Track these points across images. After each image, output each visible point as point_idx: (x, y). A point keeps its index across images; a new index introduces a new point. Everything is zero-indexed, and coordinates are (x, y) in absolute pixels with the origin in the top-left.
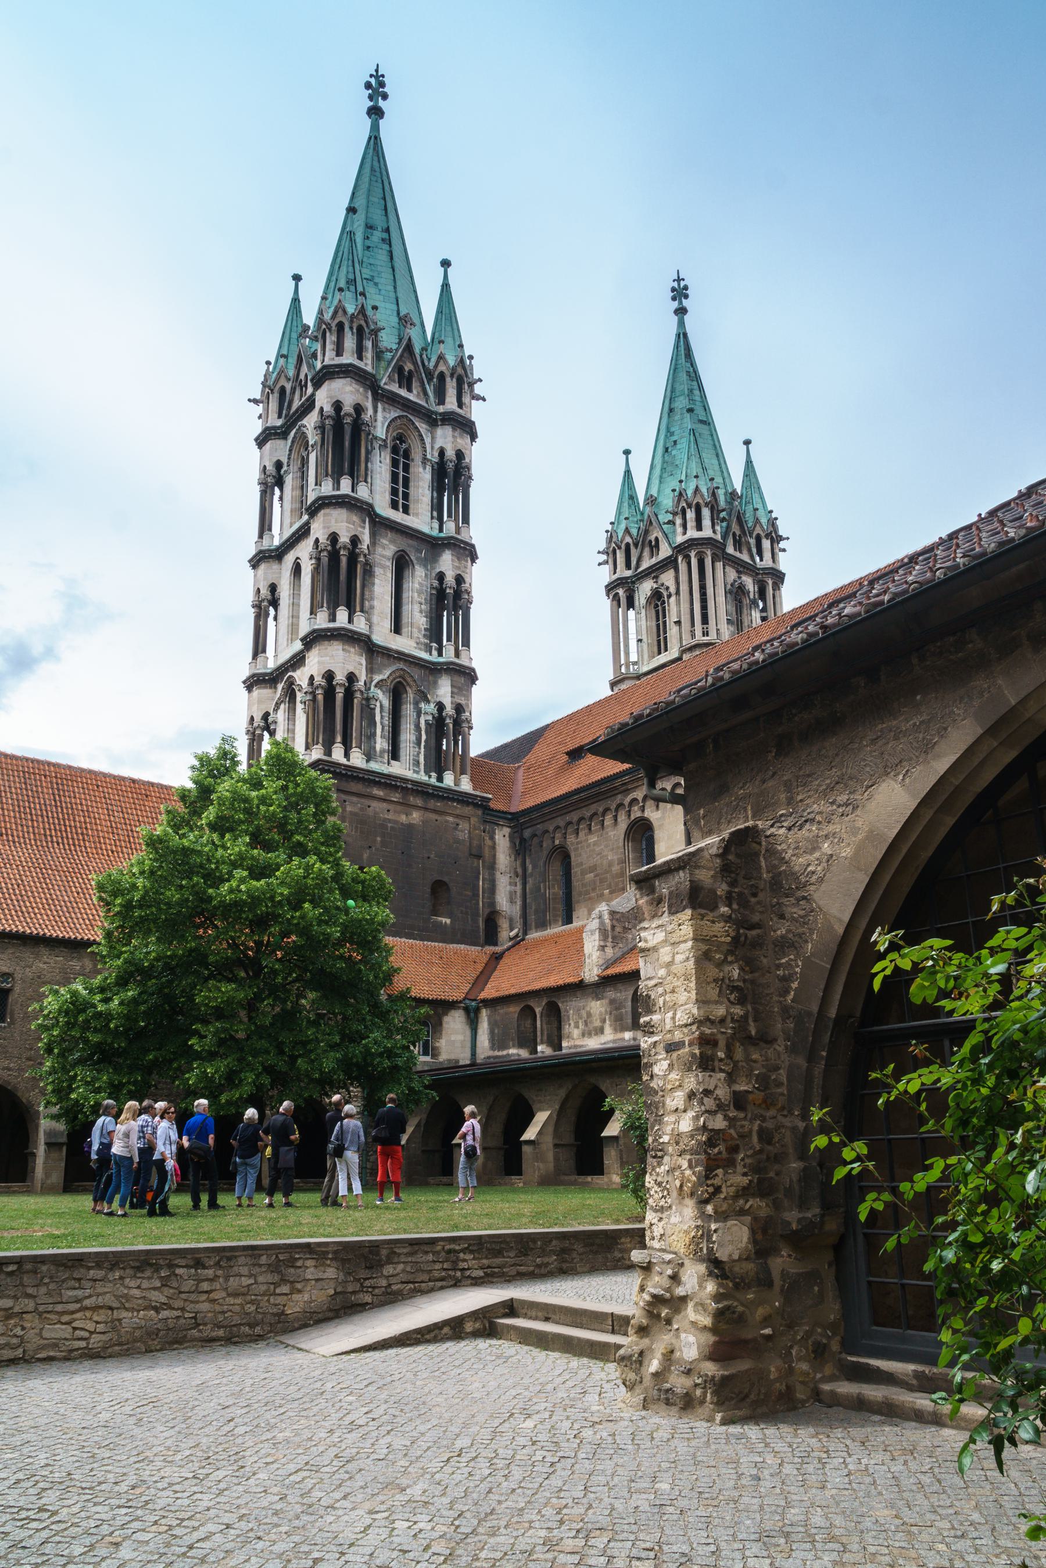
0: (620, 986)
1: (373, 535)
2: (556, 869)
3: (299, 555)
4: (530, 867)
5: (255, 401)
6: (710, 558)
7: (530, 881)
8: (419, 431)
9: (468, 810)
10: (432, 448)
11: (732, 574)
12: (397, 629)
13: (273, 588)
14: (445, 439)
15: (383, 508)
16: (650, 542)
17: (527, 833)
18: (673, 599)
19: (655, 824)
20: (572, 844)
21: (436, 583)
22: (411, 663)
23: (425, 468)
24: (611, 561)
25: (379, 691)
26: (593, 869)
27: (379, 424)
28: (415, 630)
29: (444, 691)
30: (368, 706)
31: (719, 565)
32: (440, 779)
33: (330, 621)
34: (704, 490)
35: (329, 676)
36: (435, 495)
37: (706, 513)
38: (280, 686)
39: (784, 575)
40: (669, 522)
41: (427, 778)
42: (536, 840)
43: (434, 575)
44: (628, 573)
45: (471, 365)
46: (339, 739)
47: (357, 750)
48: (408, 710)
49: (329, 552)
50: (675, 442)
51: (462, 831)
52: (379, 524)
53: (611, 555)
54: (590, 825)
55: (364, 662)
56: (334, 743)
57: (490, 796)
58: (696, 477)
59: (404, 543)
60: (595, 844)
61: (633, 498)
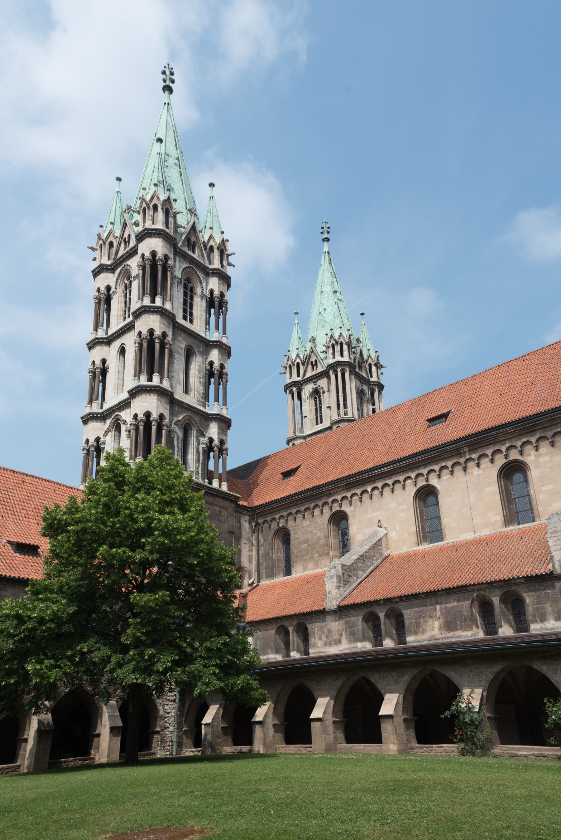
0: (353, 612)
2: (279, 544)
4: (262, 541)
7: (262, 549)
9: (227, 504)
11: (359, 384)
12: (186, 391)
13: (104, 361)
16: (312, 362)
17: (260, 521)
18: (325, 395)
19: (349, 514)
20: (292, 526)
21: (208, 368)
22: (195, 412)
25: (176, 427)
26: (306, 541)
29: (213, 430)
30: (170, 436)
31: (353, 377)
32: (210, 483)
35: (148, 415)
37: (345, 347)
39: (384, 386)
40: (323, 352)
41: (203, 482)
42: (266, 525)
43: (207, 362)
44: (299, 379)
48: (193, 441)
50: (325, 309)
51: (223, 516)
53: (288, 369)
54: (304, 515)
55: (168, 408)
57: (240, 496)
59: (192, 342)
60: (308, 526)
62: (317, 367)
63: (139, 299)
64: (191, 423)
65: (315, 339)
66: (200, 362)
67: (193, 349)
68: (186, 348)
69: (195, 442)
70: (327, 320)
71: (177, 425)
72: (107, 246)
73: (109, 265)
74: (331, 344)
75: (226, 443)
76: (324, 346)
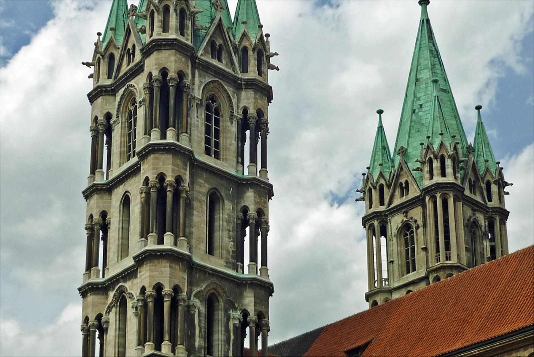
1: (192, 176)
3: (129, 189)
6: (452, 199)
8: (228, 93)
10: (238, 107)
11: (469, 212)
12: (211, 251)
13: (104, 215)
16: (401, 184)
21: (241, 215)
22: (222, 278)
23: (232, 123)
24: (367, 197)
25: (197, 300)
28: (224, 252)
33: (158, 244)
35: (159, 287)
36: (240, 144)
37: (449, 163)
38: (111, 294)
39: (509, 212)
40: (417, 169)
43: (239, 208)
46: (167, 337)
47: (182, 346)
49: (157, 188)
55: (186, 277)
56: (162, 341)
59: (216, 182)
61: (385, 148)
62: (408, 191)
63: (145, 134)
64: (218, 292)
65: (406, 150)
66: (229, 210)
67: (219, 192)
68: (209, 193)
69: (223, 318)
70: (424, 122)
71: (198, 298)
72: (107, 60)
73: (108, 86)
74: (427, 159)
75: (266, 316)
76: (417, 161)
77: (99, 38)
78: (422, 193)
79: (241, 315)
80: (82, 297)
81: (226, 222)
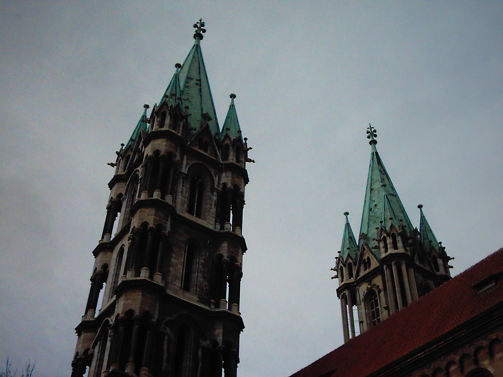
5: (112, 165)
10: (219, 183)
11: (421, 278)
14: (226, 179)
15: (181, 210)
18: (382, 294)
24: (339, 276)
27: (184, 166)
34: (397, 227)
37: (399, 239)
40: (376, 247)
45: (246, 143)
50: (376, 205)
52: (178, 220)
58: (391, 219)
61: (351, 238)
62: (370, 264)
70: (378, 215)
77: (122, 147)
78: (380, 264)
79: (211, 345)
80: (77, 335)
81: (202, 265)
